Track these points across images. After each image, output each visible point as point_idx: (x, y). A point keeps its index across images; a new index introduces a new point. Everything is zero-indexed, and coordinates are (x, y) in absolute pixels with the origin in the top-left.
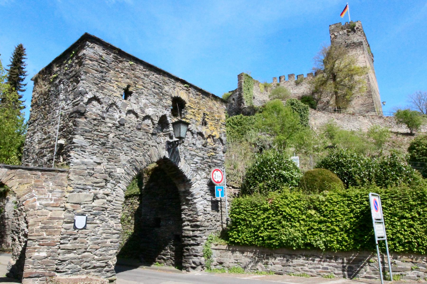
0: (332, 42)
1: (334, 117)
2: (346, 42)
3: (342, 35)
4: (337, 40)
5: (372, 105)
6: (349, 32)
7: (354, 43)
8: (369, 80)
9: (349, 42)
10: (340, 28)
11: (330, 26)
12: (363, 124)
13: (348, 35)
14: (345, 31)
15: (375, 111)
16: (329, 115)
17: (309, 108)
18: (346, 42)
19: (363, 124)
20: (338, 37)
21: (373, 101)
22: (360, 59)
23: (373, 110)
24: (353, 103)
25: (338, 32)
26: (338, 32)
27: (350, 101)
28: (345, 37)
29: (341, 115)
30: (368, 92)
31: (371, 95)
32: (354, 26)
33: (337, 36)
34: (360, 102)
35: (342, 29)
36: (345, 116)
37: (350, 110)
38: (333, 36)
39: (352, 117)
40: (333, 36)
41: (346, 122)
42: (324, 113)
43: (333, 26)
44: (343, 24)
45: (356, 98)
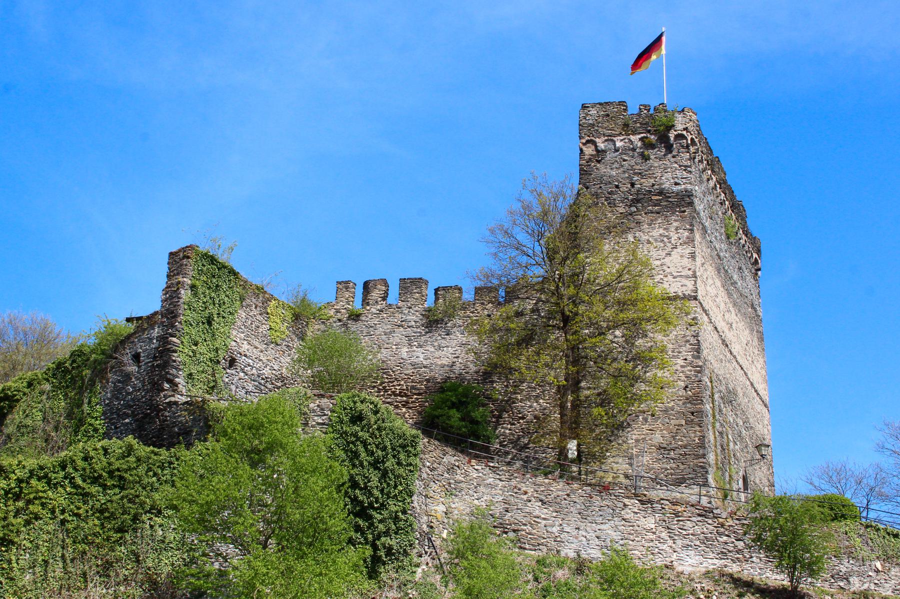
0: (584, 173)
1: (530, 491)
2: (633, 185)
3: (625, 150)
4: (603, 169)
5: (698, 457)
7: (661, 192)
8: (698, 350)
9: (647, 183)
10: (620, 122)
11: (584, 107)
12: (638, 534)
13: (646, 158)
14: (635, 138)
15: (706, 484)
16: (514, 483)
17: (423, 441)
18: (633, 185)
19: (638, 534)
20: (609, 156)
21: (703, 438)
22: (675, 261)
23: (699, 476)
24: (632, 436)
25: (610, 140)
26: (610, 140)
28: (631, 161)
29: (558, 488)
31: (700, 413)
32: (670, 127)
33: (604, 151)
34: (658, 438)
35: (627, 128)
36: (573, 491)
37: (616, 466)
38: (589, 150)
39: (597, 501)
40: (589, 150)
41: (574, 518)
42: (494, 470)
43: (593, 112)
44: (633, 109)
45: (646, 420)
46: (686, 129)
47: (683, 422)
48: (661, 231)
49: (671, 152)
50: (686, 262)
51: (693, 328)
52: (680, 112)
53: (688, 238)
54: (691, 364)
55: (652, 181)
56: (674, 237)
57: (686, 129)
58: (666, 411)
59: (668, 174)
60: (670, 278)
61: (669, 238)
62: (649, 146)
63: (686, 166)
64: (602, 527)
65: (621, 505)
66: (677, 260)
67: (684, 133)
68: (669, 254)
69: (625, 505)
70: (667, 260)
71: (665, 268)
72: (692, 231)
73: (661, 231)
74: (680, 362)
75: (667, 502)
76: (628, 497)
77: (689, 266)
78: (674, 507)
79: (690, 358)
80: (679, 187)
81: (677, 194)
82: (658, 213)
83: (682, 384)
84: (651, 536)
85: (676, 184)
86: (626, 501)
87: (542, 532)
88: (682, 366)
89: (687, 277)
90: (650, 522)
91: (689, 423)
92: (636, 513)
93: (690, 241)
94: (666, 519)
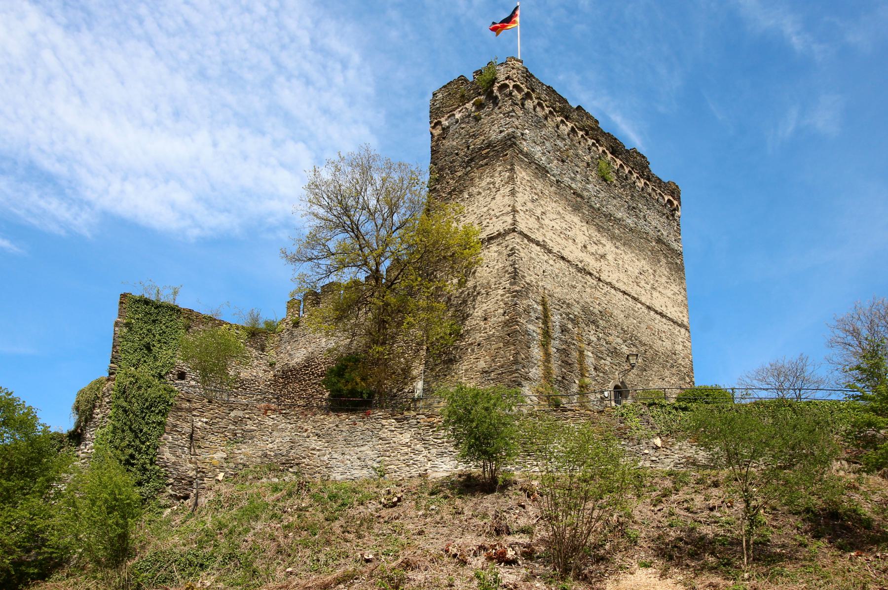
6: (480, 106)
7: (489, 145)
13: (477, 119)
27: (451, 361)
30: (506, 324)
32: (494, 81)
34: (482, 364)
36: (341, 421)
41: (340, 445)
46: (508, 78)
47: (501, 345)
48: (488, 180)
49: (497, 104)
50: (507, 200)
51: (511, 258)
52: (502, 64)
53: (509, 177)
54: (509, 291)
55: (483, 137)
56: (498, 180)
57: (508, 78)
58: (488, 338)
59: (495, 127)
60: (494, 219)
61: (494, 183)
62: (480, 106)
63: (509, 113)
64: (362, 449)
65: (379, 426)
66: (502, 200)
67: (507, 82)
68: (494, 198)
69: (383, 426)
70: (492, 205)
71: (491, 211)
72: (512, 170)
73: (488, 180)
74: (501, 292)
75: (423, 416)
76: (386, 418)
77: (509, 203)
78: (429, 420)
79: (508, 286)
80: (503, 134)
81: (501, 141)
82: (487, 164)
83: (501, 311)
84: (405, 449)
85: (501, 132)
86: (384, 422)
87: (315, 461)
88: (502, 295)
89: (508, 213)
90: (406, 437)
91: (507, 344)
92: (393, 431)
93: (511, 179)
94: (421, 431)
